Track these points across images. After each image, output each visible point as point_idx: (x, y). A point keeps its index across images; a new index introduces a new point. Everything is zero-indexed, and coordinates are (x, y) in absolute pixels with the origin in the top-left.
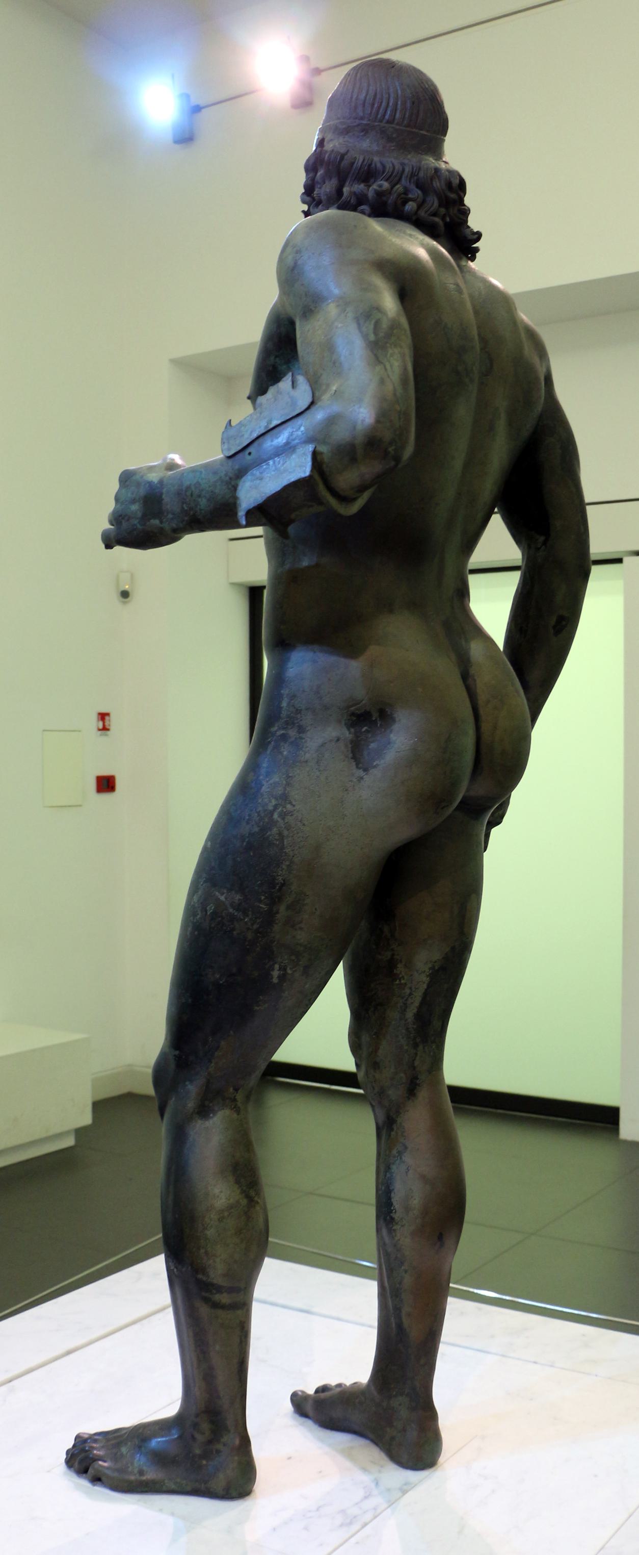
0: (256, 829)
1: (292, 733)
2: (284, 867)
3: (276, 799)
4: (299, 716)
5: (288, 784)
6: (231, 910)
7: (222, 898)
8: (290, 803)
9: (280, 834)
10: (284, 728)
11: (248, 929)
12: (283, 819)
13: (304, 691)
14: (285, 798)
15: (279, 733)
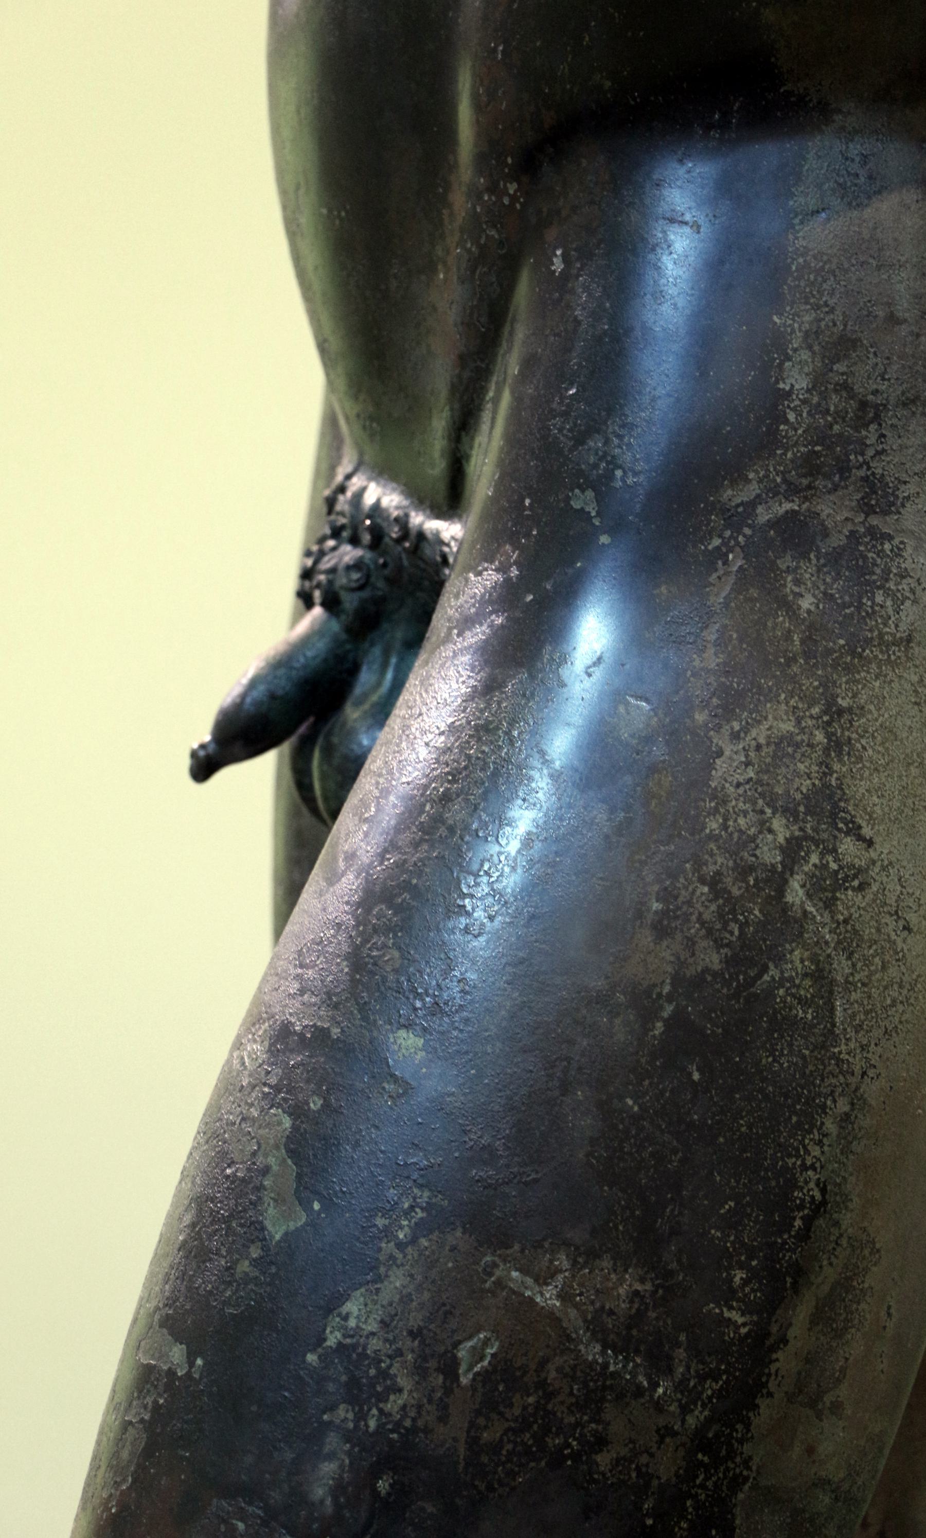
0: (714, 960)
1: (835, 511)
2: (830, 1126)
3: (790, 812)
4: (871, 435)
5: (836, 745)
6: (592, 1352)
7: (548, 1297)
8: (854, 831)
9: (820, 975)
10: (792, 490)
11: (665, 1432)
12: (829, 905)
13: (893, 320)
14: (827, 810)
15: (763, 515)
